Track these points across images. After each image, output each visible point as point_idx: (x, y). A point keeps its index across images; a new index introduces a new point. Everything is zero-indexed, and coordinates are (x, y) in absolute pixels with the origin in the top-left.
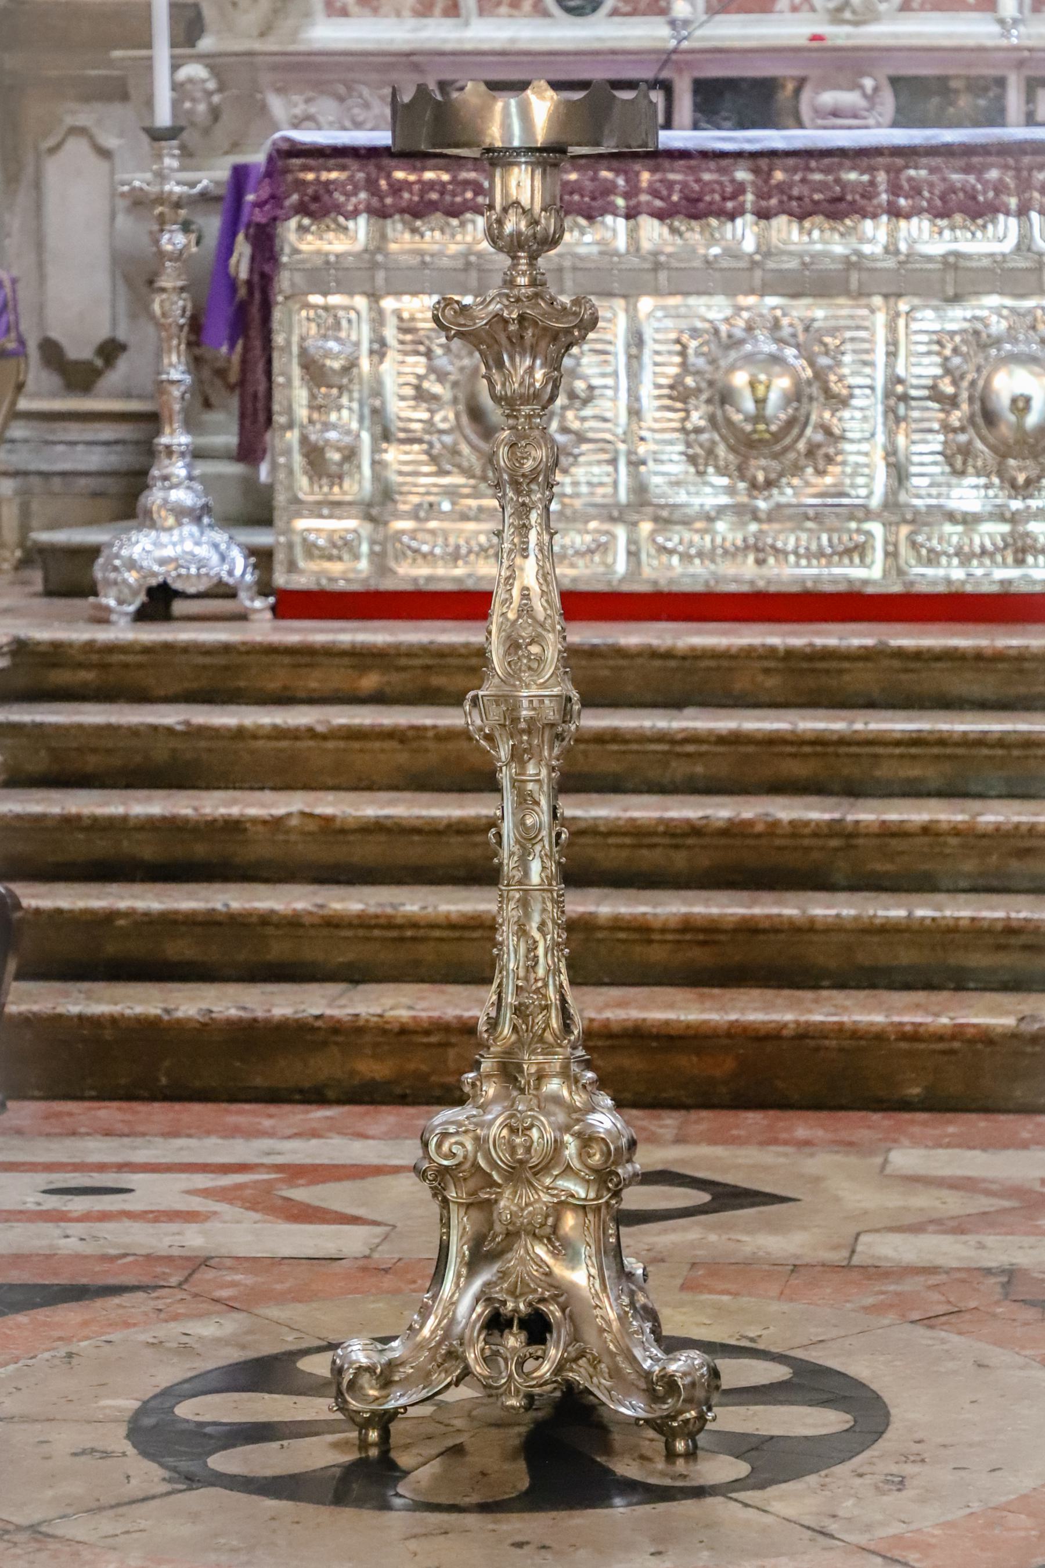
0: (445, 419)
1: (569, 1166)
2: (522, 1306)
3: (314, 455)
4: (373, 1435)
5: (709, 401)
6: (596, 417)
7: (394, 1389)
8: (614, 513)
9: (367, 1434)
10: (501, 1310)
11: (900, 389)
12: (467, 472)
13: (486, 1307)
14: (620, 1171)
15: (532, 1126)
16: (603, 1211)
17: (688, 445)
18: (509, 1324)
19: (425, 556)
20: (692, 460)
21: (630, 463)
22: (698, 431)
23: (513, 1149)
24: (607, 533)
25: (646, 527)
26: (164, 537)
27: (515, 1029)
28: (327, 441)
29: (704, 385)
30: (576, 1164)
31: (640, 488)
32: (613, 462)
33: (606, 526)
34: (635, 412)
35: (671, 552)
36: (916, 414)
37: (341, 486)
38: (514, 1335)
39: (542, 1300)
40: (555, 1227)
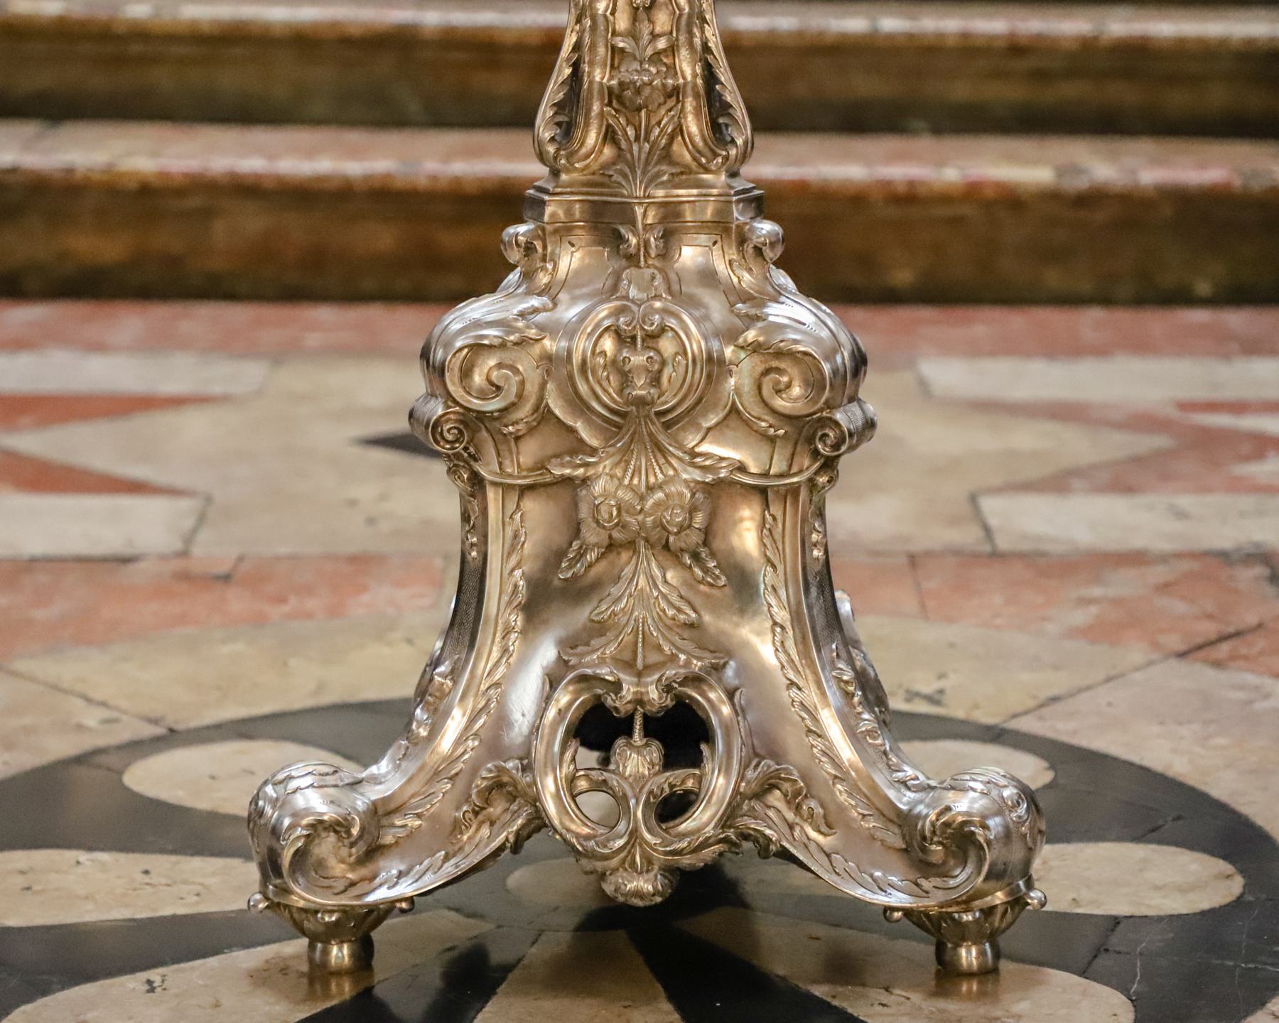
1: (734, 410)
2: (653, 694)
4: (340, 954)
7: (382, 863)
9: (326, 952)
10: (609, 701)
13: (577, 694)
14: (839, 416)
15: (663, 330)
16: (803, 494)
18: (624, 727)
23: (625, 377)
27: (610, 135)
30: (751, 407)
38: (638, 750)
39: (695, 680)
40: (708, 533)
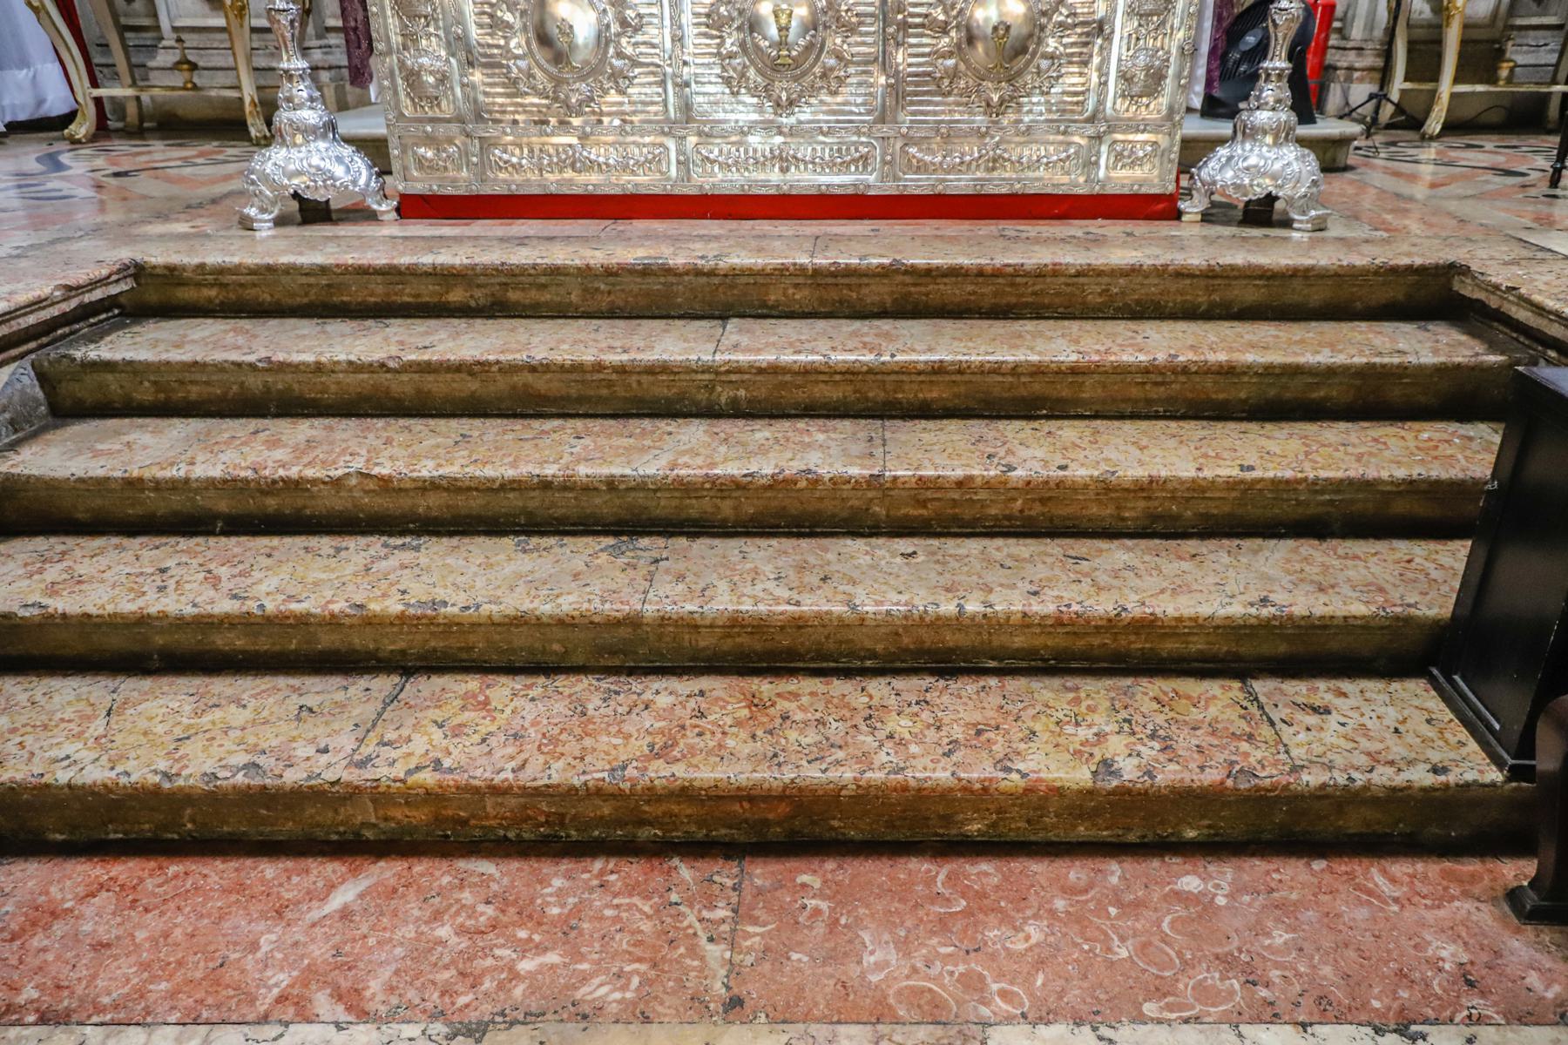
0: (519, 46)
3: (412, 77)
5: (739, 29)
6: (644, 43)
8: (668, 128)
11: (900, 17)
12: (542, 94)
17: (724, 69)
19: (513, 166)
20: (727, 81)
21: (676, 85)
22: (731, 56)
24: (661, 145)
25: (692, 140)
26: (294, 153)
28: (421, 66)
29: (735, 14)
31: (687, 107)
32: (663, 83)
33: (659, 139)
34: (678, 40)
35: (713, 162)
36: (913, 41)
37: (439, 105)
